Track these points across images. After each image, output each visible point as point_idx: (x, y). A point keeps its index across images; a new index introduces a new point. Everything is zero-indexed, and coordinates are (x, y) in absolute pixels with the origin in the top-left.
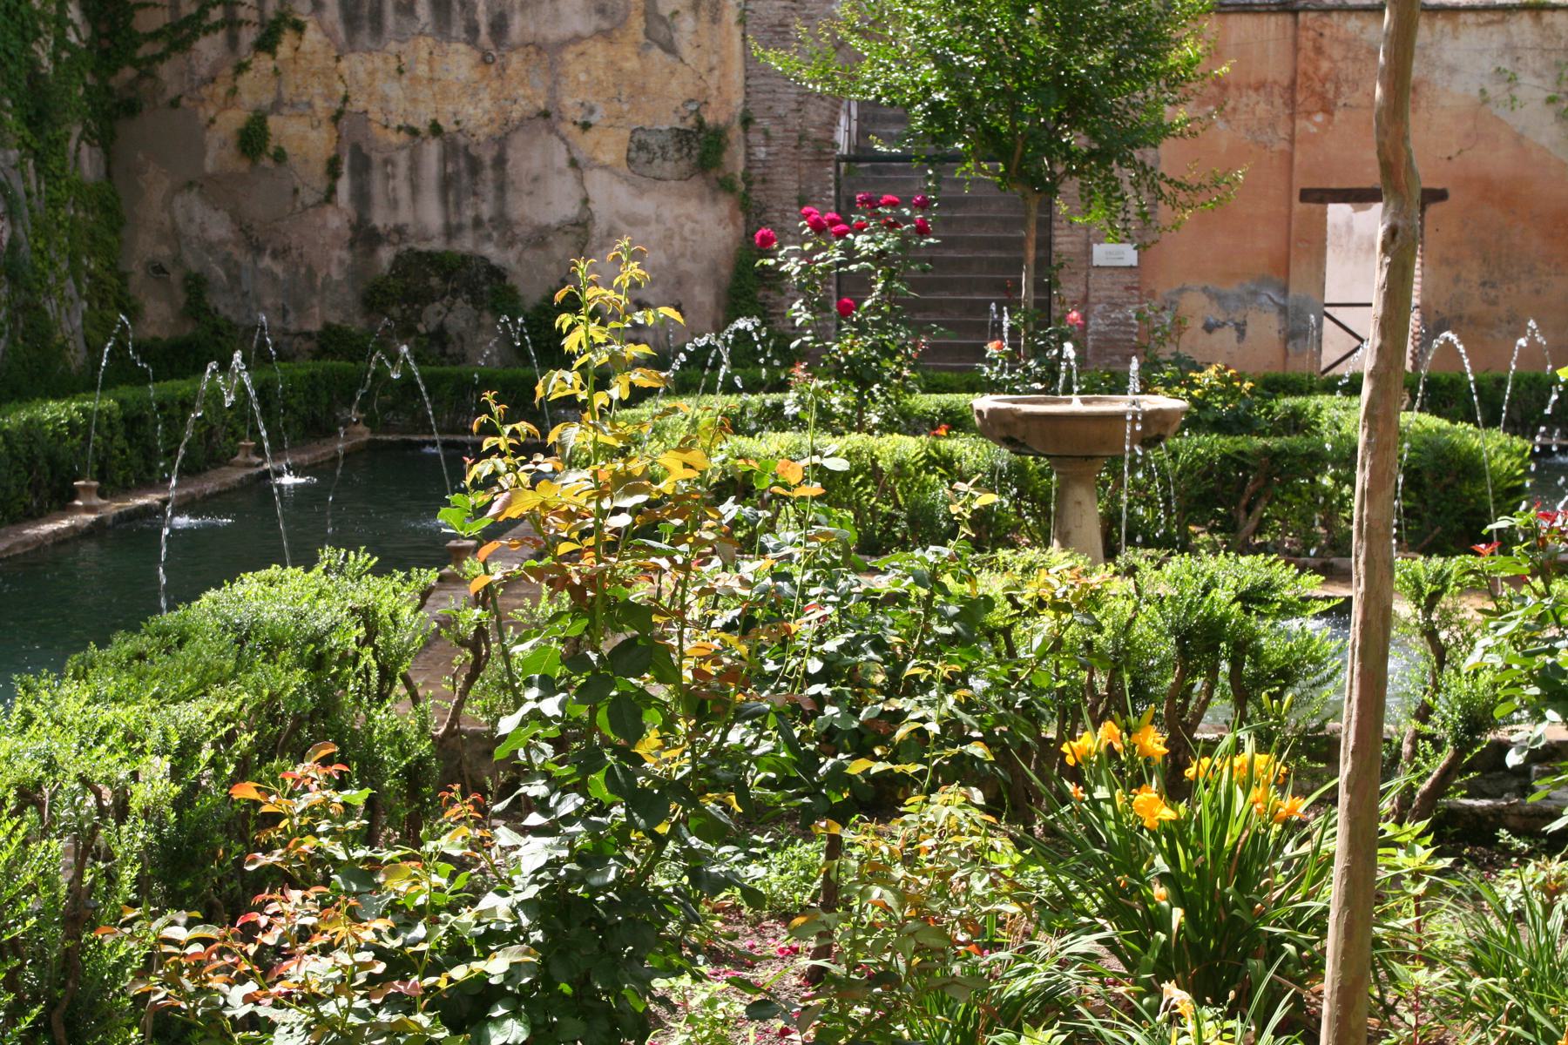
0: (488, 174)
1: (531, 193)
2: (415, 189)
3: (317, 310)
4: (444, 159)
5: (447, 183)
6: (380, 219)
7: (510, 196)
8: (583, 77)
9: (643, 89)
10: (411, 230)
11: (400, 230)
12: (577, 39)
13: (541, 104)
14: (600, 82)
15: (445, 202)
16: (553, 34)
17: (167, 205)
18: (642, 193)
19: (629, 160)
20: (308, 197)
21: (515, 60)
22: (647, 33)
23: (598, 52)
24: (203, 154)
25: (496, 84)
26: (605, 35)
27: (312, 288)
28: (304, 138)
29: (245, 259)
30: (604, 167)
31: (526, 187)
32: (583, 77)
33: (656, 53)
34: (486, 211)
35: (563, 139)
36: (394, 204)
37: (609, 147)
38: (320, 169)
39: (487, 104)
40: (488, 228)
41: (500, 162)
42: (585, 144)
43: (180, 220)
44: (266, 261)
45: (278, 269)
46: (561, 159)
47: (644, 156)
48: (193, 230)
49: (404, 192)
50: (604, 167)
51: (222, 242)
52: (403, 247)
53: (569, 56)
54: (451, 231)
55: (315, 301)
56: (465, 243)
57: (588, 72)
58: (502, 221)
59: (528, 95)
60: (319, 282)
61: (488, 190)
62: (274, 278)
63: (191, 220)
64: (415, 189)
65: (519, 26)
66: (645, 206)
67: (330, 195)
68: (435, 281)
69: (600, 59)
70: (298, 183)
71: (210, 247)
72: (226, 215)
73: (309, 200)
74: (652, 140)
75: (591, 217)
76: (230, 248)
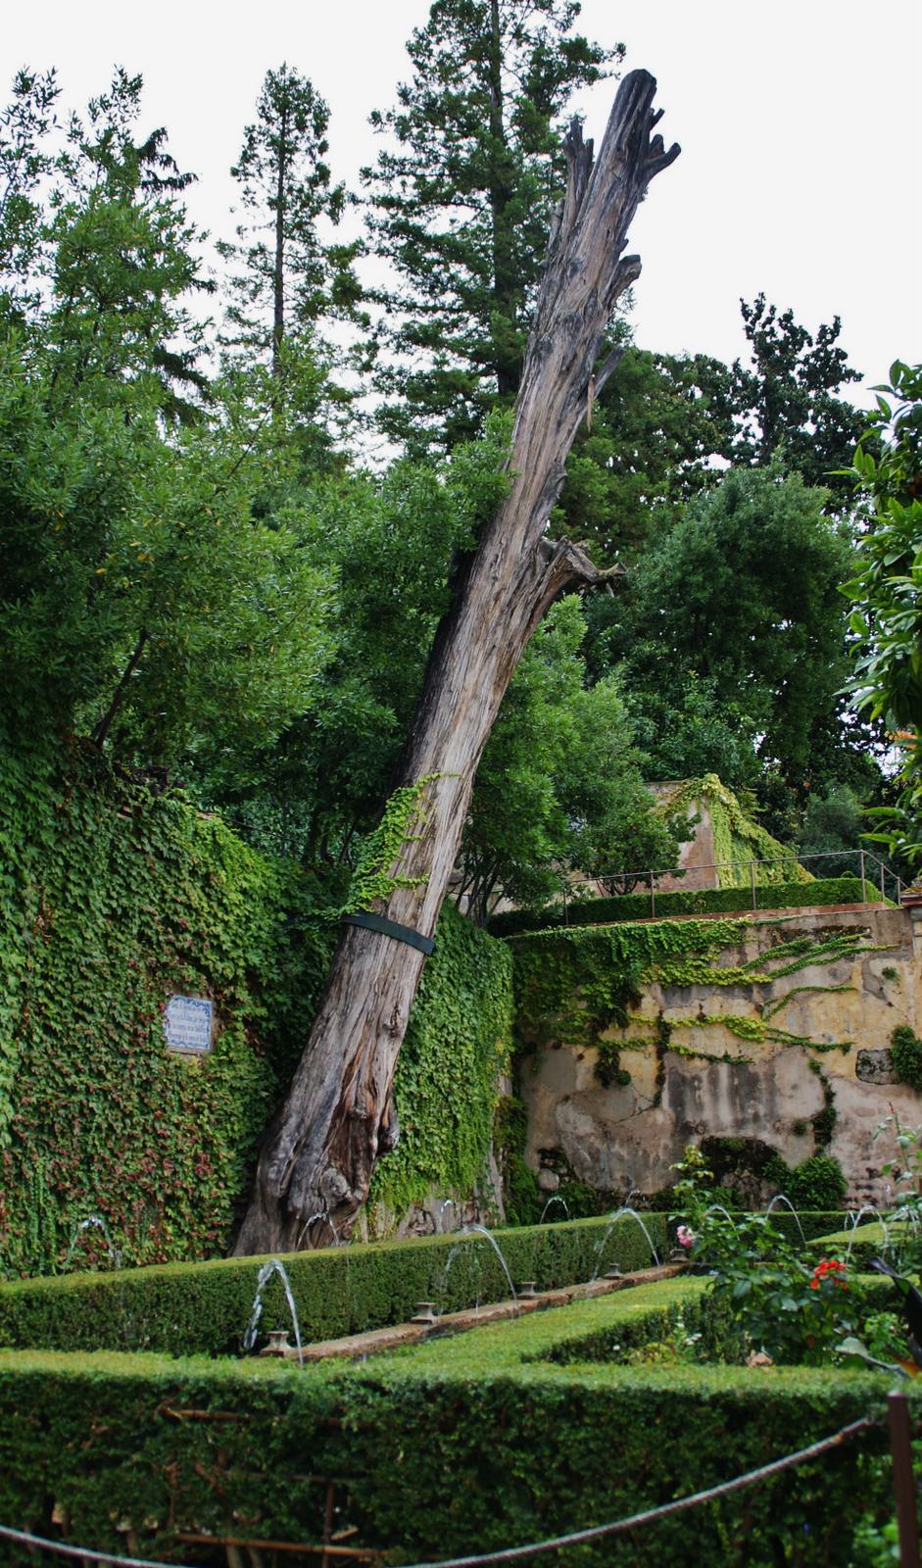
0: (763, 1085)
1: (791, 1097)
2: (715, 1096)
3: (650, 1180)
4: (732, 1076)
5: (734, 1091)
6: (690, 1117)
7: (778, 1099)
8: (823, 1018)
9: (864, 1024)
10: (711, 1125)
14: (834, 1021)
15: (733, 1104)
17: (552, 1113)
18: (868, 1094)
19: (858, 1073)
20: (644, 1104)
24: (575, 1078)
27: (646, 1164)
28: (640, 1065)
29: (603, 1147)
31: (788, 1091)
33: (872, 999)
34: (762, 1110)
36: (700, 1107)
38: (649, 1089)
40: (763, 1121)
41: (771, 1077)
43: (560, 1121)
44: (616, 1148)
45: (624, 1153)
47: (867, 1069)
48: (569, 1128)
49: (706, 1098)
51: (589, 1135)
52: (707, 1136)
54: (739, 1124)
55: (648, 1174)
56: (748, 1132)
57: (826, 1014)
58: (774, 1117)
60: (651, 1160)
61: (765, 1097)
62: (621, 1159)
63: (567, 1122)
64: (715, 1096)
66: (871, 1102)
67: (657, 1101)
69: (834, 1005)
70: (636, 1095)
71: (580, 1139)
72: (590, 1118)
73: (644, 1107)
74: (875, 1058)
75: (834, 1114)
76: (592, 1139)
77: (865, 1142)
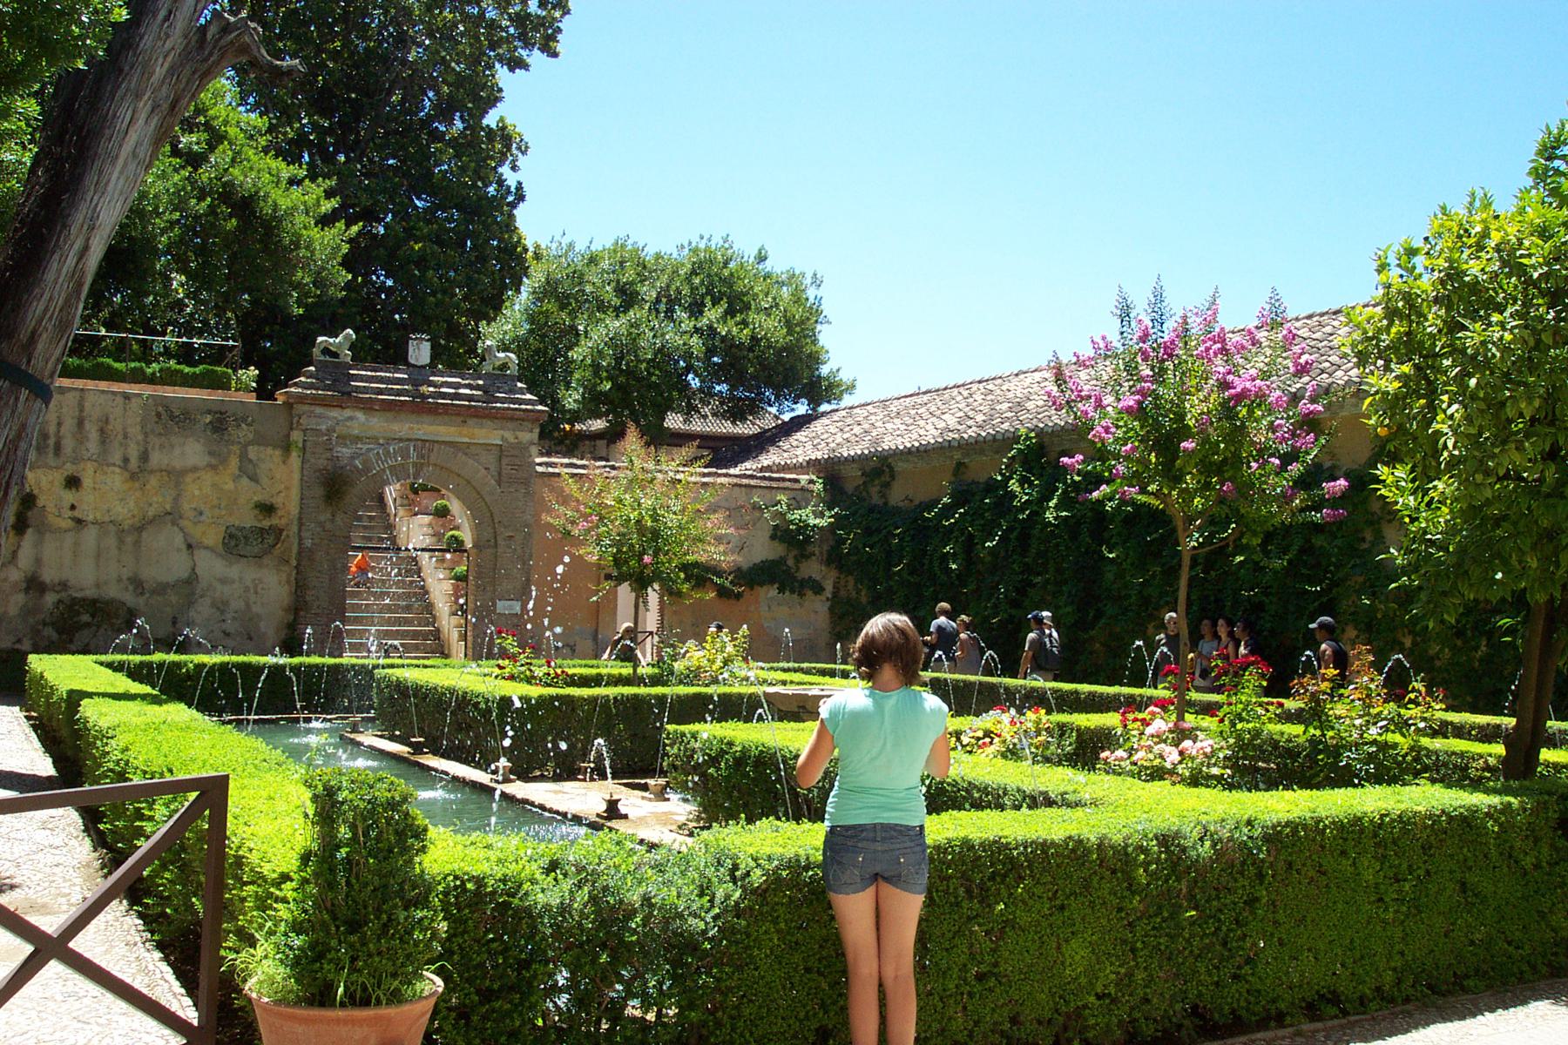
11: (64, 585)
12: (195, 469)
13: (168, 507)
16: (178, 464)
21: (154, 481)
22: (240, 469)
23: (208, 477)
25: (138, 494)
26: (213, 467)
30: (207, 548)
32: (197, 493)
33: (245, 481)
35: (181, 529)
37: (213, 537)
39: (132, 504)
42: (196, 532)
46: (179, 540)
50: (207, 548)
53: (189, 478)
59: (158, 499)
65: (156, 458)
68: (86, 618)
77: (221, 606)
